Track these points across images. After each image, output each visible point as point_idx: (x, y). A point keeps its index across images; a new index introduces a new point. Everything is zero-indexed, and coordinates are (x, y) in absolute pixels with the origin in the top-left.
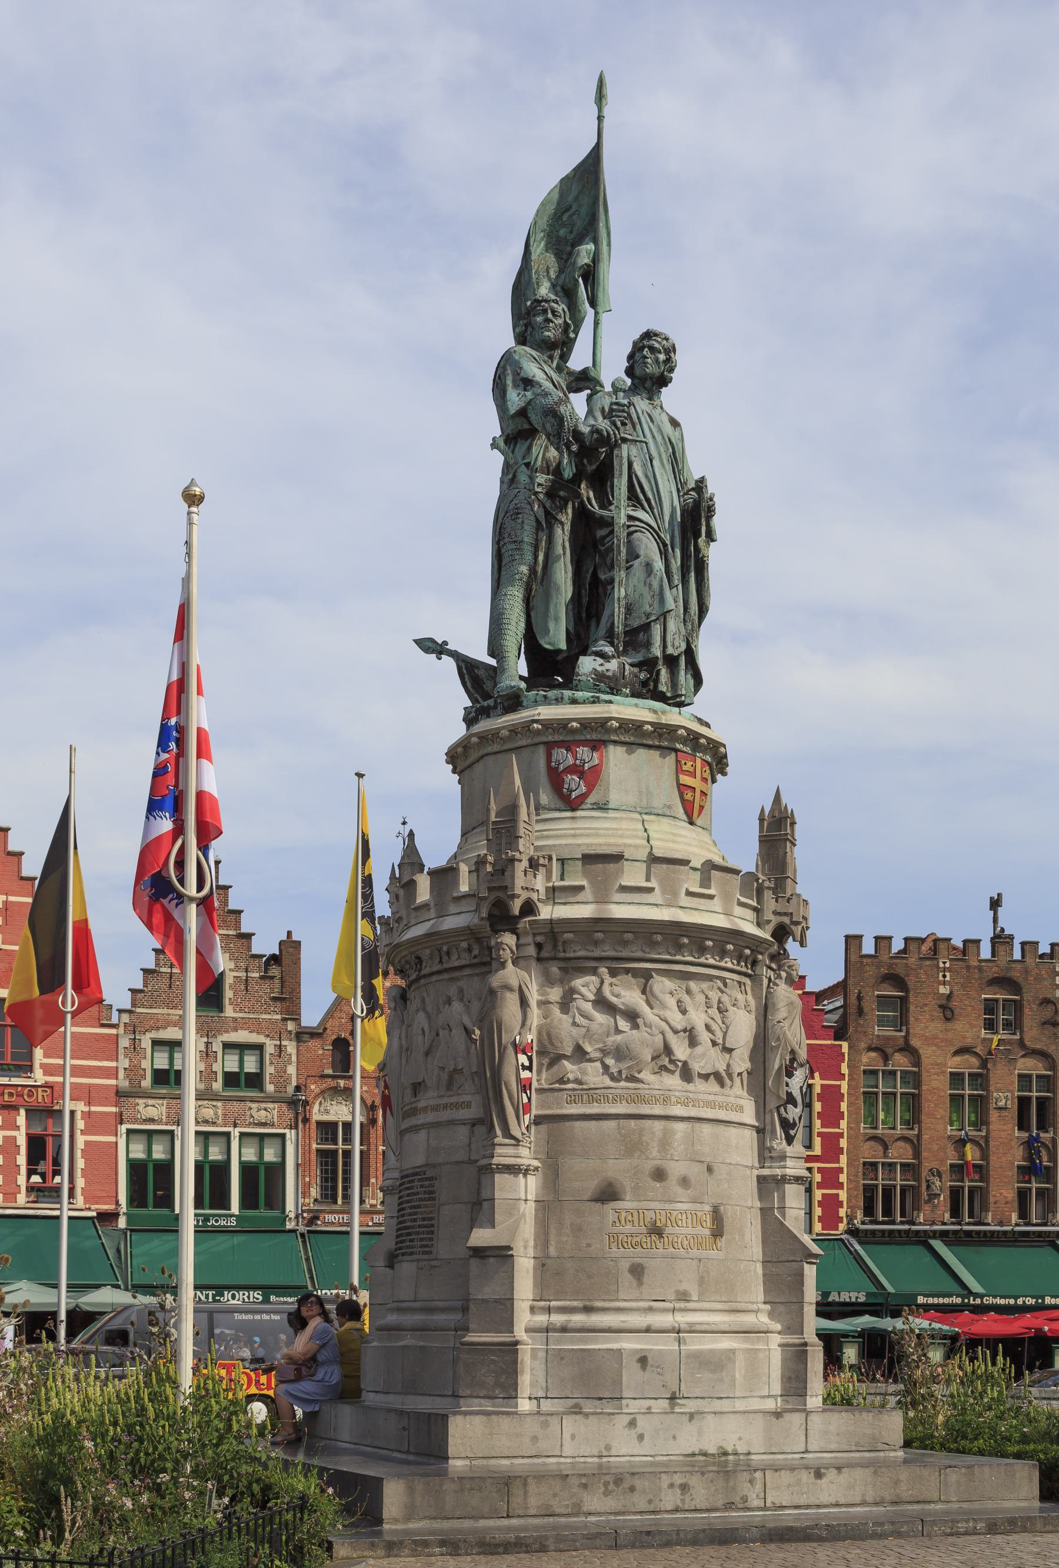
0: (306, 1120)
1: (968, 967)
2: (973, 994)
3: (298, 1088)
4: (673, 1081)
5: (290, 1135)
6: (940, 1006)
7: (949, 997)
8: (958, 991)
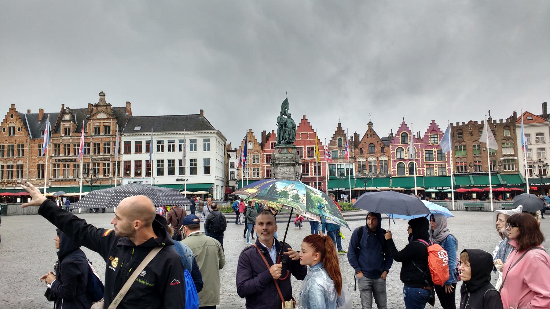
0: (356, 161)
1: (475, 126)
2: (477, 131)
3: (354, 156)
4: (286, 175)
5: (354, 164)
6: (470, 133)
7: (472, 132)
8: (473, 130)
